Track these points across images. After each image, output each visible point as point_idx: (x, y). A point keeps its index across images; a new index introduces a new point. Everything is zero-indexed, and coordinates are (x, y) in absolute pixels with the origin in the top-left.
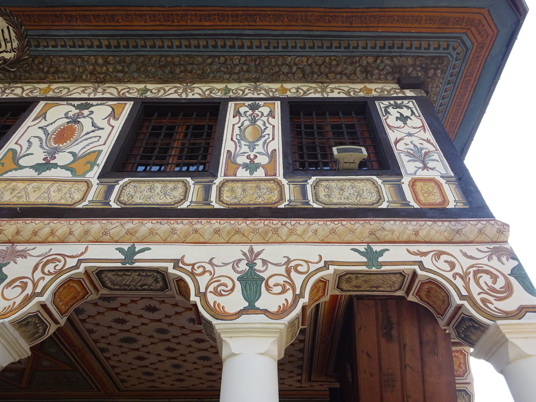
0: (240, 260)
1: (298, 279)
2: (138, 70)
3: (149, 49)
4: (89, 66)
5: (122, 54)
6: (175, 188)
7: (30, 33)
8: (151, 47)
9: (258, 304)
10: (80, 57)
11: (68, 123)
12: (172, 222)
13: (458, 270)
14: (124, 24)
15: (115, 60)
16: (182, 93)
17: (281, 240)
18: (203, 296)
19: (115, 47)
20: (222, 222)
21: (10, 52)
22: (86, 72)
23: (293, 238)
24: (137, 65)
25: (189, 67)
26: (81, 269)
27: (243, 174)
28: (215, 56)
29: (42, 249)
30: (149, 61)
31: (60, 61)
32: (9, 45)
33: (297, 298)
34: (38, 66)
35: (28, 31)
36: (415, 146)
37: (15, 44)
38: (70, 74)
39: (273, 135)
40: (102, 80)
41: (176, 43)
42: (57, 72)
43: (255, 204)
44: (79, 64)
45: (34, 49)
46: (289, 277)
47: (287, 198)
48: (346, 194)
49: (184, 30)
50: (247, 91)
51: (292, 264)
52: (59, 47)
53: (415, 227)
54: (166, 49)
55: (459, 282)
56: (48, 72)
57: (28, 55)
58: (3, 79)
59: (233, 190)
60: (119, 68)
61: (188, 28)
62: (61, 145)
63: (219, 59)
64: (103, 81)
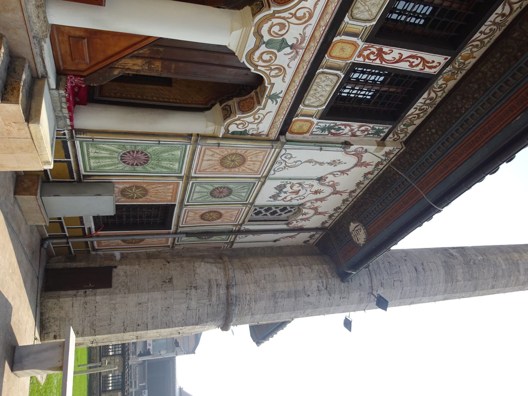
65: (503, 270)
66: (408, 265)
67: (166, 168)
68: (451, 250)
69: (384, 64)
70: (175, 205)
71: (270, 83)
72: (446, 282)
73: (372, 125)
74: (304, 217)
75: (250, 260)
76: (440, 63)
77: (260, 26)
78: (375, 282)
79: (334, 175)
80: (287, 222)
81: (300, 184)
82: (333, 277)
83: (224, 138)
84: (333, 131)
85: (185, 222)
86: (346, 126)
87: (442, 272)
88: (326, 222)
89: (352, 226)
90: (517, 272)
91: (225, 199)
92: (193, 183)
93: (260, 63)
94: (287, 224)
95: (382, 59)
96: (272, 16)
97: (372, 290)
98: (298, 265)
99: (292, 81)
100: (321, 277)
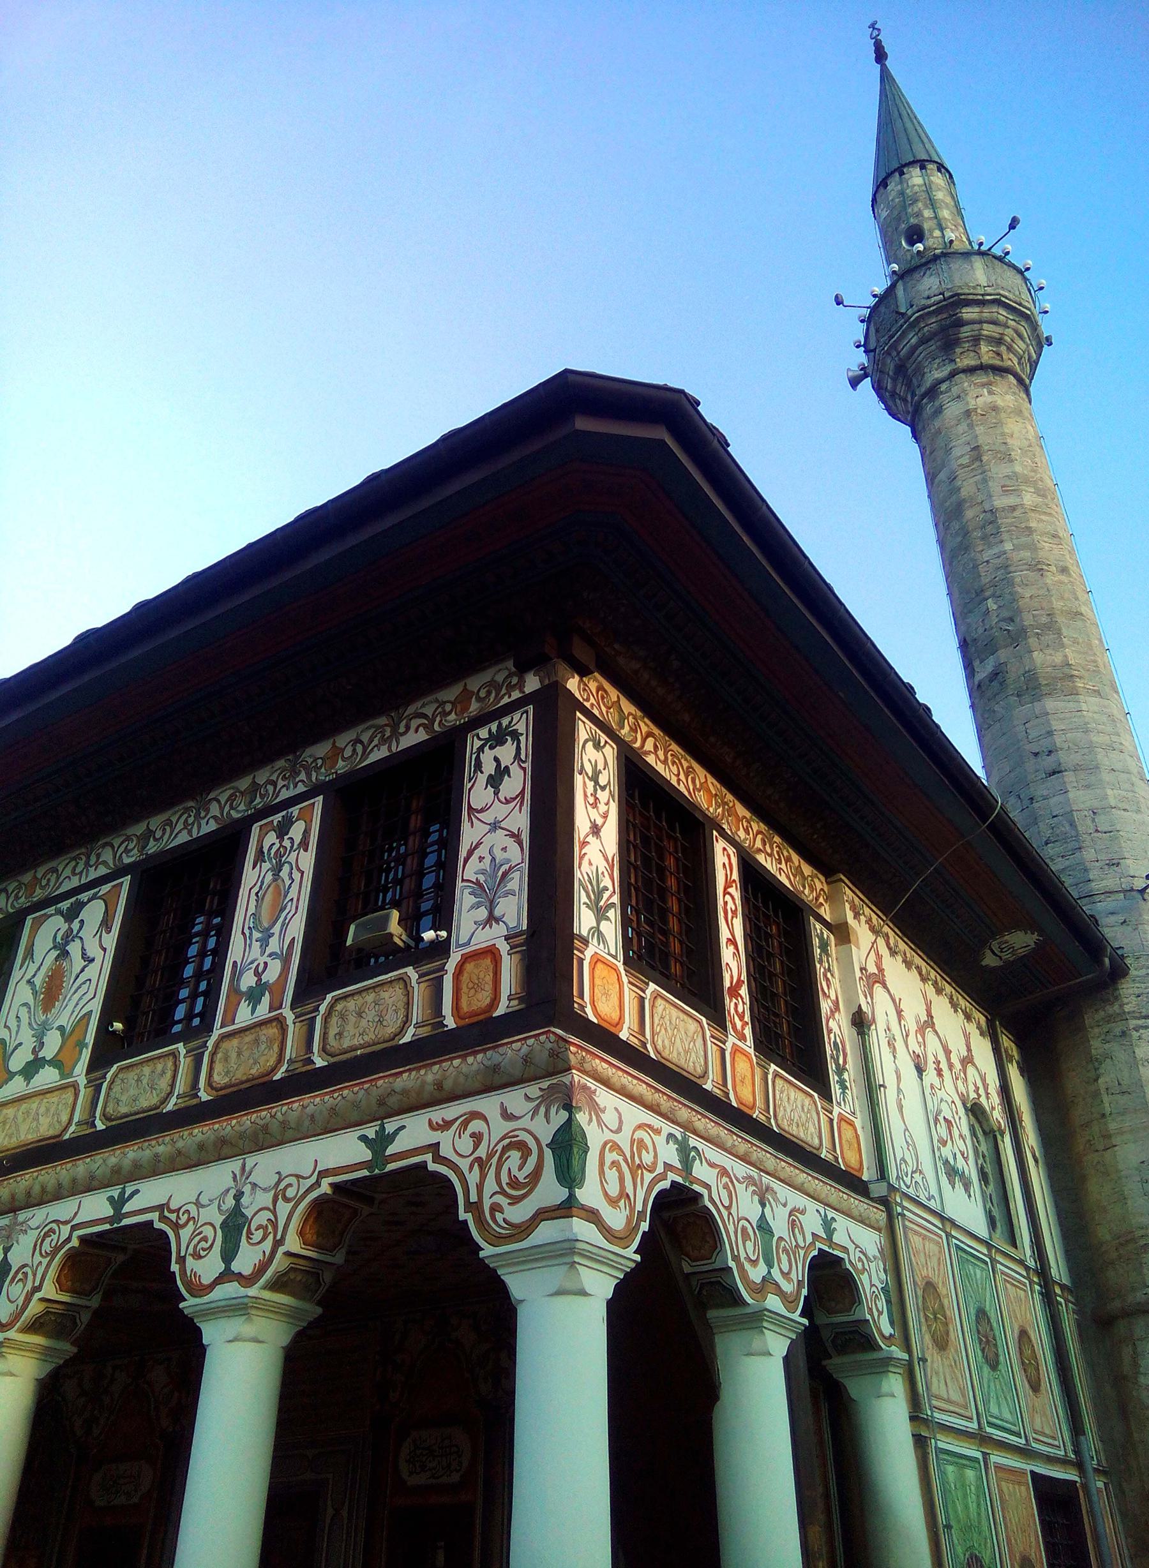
0: (228, 1191)
1: (283, 1208)
6: (163, 1072)
9: (236, 1266)
11: (56, 959)
12: (154, 1143)
13: (482, 1152)
16: (193, 824)
17: (275, 1141)
18: (182, 1260)
20: (206, 1129)
23: (289, 1134)
26: (75, 1242)
27: (244, 1015)
29: (38, 1216)
33: (278, 1243)
36: (494, 859)
39: (298, 900)
43: (247, 1081)
46: (274, 1213)
47: (287, 1058)
48: (364, 1023)
50: (281, 783)
51: (282, 1186)
53: (437, 1077)
55: (473, 1178)
59: (226, 1059)
65: (1016, 548)
66: (1045, 793)
67: (979, 1505)
68: (979, 677)
69: (744, 977)
70: (1032, 1472)
71: (813, 1243)
72: (1074, 692)
73: (818, 966)
74: (981, 1091)
75: (1103, 1233)
76: (724, 849)
77: (752, 1286)
78: (1110, 881)
79: (907, 1036)
80: (999, 1137)
81: (936, 1120)
82: (1116, 998)
83: (908, 1348)
84: (841, 1061)
85: (1054, 1438)
86: (830, 1031)
87: (1050, 704)
88: (979, 1027)
89: (990, 960)
90: (1016, 514)
91: (995, 1325)
92: (991, 1425)
93: (793, 1275)
94: (1002, 1134)
95: (740, 983)
96: (736, 1258)
97: (1132, 890)
98: (1097, 1094)
99: (800, 1189)
100: (1124, 1034)
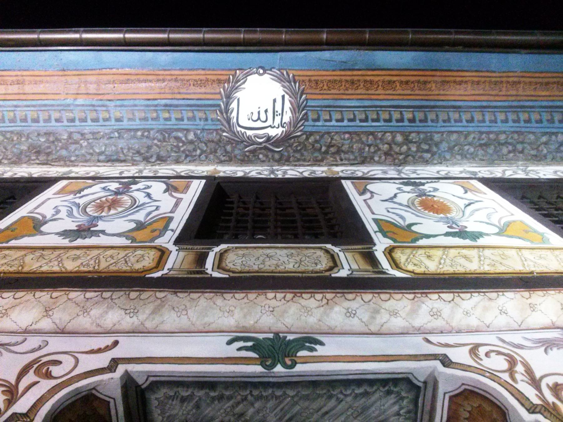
2: (451, 149)
3: (465, 123)
4: (383, 145)
5: (429, 129)
7: (310, 103)
8: (467, 121)
10: (372, 133)
14: (437, 93)
15: (420, 139)
19: (421, 121)
21: (277, 128)
22: (379, 153)
24: (448, 143)
25: (520, 147)
28: (553, 133)
30: (466, 138)
31: (344, 139)
32: (278, 119)
34: (313, 146)
35: (309, 101)
37: (287, 117)
38: (357, 154)
40: (402, 161)
41: (501, 117)
42: (339, 151)
44: (370, 142)
45: (311, 123)
49: (512, 101)
52: (346, 121)
54: (487, 123)
56: (326, 152)
57: (301, 131)
58: (263, 161)
60: (426, 147)
61: (519, 98)
62: (449, 215)
63: (557, 136)
64: (404, 163)
